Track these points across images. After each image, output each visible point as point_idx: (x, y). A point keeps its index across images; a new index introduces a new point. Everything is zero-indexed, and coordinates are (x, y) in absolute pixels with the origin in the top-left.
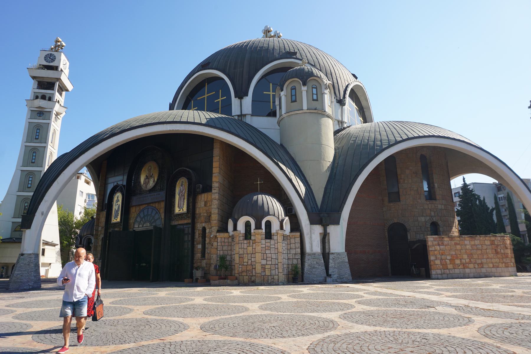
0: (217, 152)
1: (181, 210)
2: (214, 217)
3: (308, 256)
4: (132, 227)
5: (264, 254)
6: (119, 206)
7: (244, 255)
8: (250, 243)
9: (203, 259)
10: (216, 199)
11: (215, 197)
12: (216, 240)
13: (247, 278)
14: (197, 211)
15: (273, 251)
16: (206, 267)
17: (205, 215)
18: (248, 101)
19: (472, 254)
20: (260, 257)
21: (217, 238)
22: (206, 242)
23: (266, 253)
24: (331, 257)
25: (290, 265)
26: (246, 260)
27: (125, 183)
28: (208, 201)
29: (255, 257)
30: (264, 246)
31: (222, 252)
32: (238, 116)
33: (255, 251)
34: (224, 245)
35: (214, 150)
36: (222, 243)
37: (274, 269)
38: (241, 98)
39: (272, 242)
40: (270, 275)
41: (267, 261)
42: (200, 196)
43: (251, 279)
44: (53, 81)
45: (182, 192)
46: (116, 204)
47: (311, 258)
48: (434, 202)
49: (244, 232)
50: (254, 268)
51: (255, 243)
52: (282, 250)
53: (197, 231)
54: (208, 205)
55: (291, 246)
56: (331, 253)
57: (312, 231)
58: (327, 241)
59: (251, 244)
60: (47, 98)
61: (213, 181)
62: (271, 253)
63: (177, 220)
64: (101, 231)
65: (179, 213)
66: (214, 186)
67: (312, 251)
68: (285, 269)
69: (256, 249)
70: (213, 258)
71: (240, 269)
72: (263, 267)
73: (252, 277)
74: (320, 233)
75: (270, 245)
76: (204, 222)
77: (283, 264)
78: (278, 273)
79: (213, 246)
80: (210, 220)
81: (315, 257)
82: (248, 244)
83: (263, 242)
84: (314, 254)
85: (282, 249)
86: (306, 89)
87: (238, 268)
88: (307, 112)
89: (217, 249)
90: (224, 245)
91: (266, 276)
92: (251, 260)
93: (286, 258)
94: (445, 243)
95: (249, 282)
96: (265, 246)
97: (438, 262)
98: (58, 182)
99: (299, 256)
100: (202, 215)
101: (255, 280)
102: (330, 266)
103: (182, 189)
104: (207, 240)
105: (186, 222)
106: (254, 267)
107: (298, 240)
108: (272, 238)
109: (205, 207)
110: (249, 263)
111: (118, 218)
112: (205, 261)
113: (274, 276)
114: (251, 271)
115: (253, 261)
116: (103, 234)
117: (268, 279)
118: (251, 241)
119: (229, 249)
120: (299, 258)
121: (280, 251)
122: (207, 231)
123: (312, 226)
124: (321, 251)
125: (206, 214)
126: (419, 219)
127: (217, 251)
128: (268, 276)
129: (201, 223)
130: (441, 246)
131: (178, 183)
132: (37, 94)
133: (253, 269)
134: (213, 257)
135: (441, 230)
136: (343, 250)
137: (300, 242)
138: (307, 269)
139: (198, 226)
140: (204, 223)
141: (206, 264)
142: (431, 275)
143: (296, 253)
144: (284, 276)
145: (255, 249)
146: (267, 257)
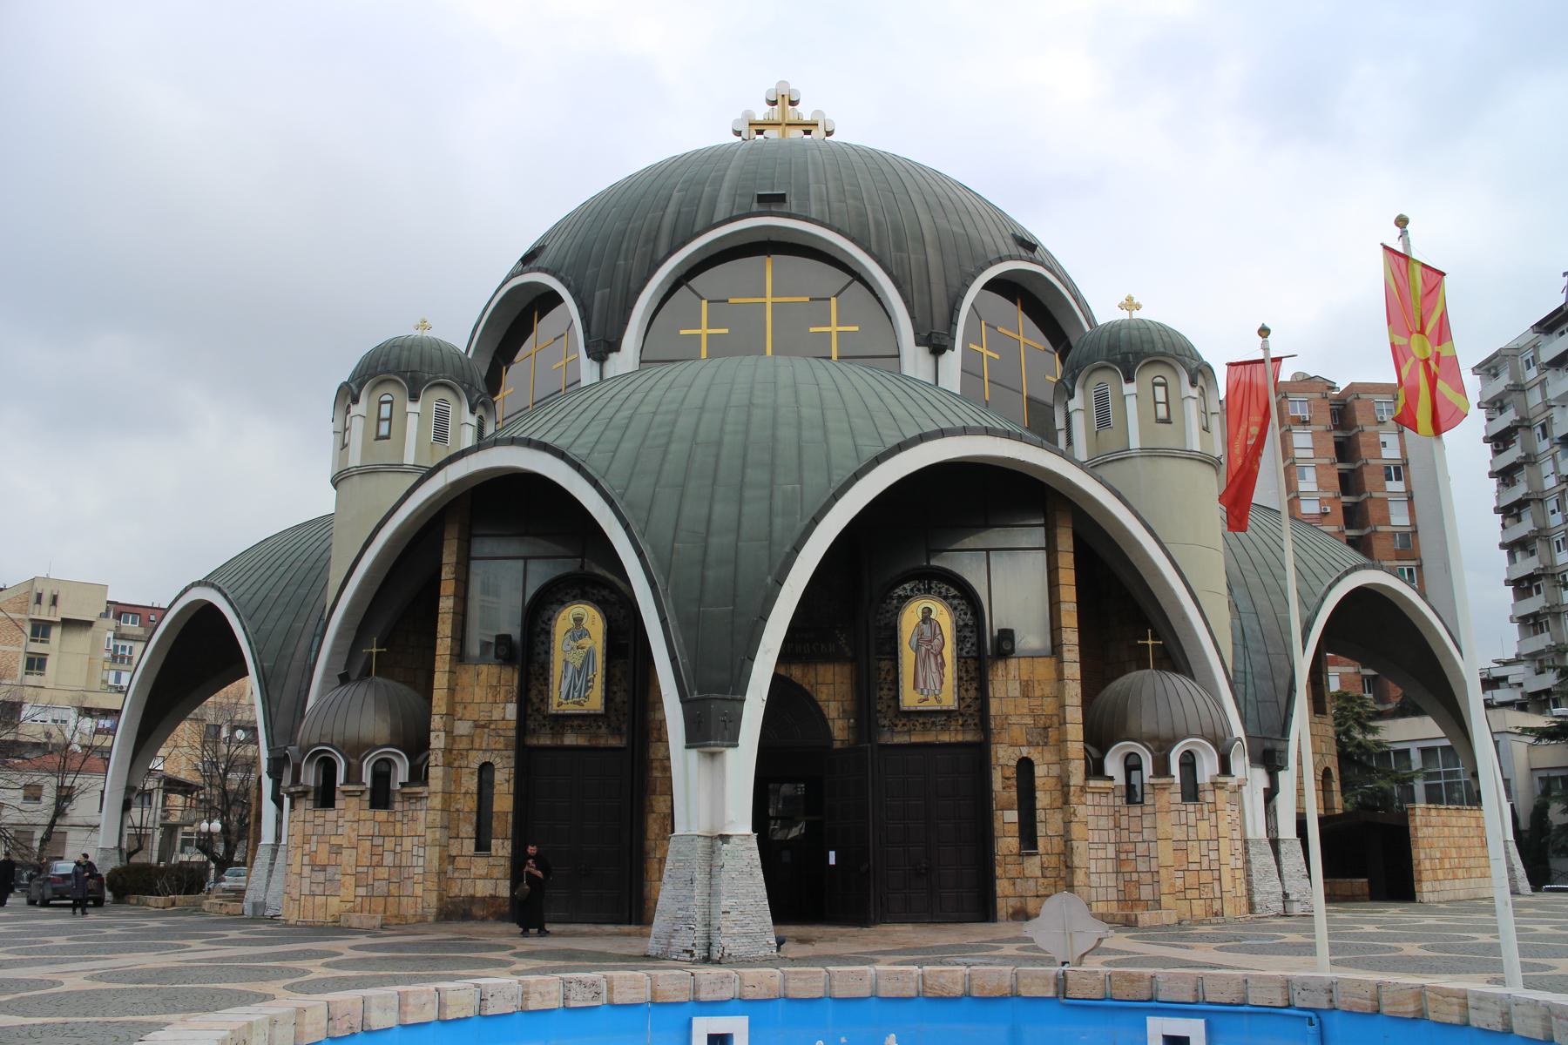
1: (931, 698)
6: (589, 656)
8: (1202, 810)
9: (1031, 854)
11: (1072, 674)
12: (1083, 799)
16: (1044, 877)
19: (1460, 847)
21: (1086, 792)
22: (1039, 804)
24: (1283, 848)
26: (1194, 857)
28: (1036, 683)
31: (1097, 832)
33: (1218, 833)
35: (1058, 531)
38: (937, 350)
42: (1001, 665)
43: (1211, 906)
45: (931, 641)
46: (572, 643)
53: (999, 768)
54: (1036, 695)
58: (1271, 808)
59: (1206, 813)
63: (909, 732)
64: (471, 737)
65: (919, 708)
71: (1179, 882)
74: (1264, 789)
76: (1025, 744)
79: (1076, 816)
80: (1047, 737)
82: (1198, 815)
87: (1170, 879)
97: (1427, 864)
98: (790, 585)
100: (1013, 720)
102: (1284, 872)
104: (1042, 799)
105: (945, 738)
106: (1216, 874)
109: (1027, 699)
110: (1205, 865)
111: (588, 697)
112: (1037, 859)
116: (434, 749)
118: (1205, 807)
119: (1111, 825)
122: (1040, 771)
123: (1253, 769)
125: (1029, 721)
129: (1011, 746)
135: (1334, 789)
139: (1001, 753)
141: (1042, 867)
142: (1417, 894)
145: (1217, 826)
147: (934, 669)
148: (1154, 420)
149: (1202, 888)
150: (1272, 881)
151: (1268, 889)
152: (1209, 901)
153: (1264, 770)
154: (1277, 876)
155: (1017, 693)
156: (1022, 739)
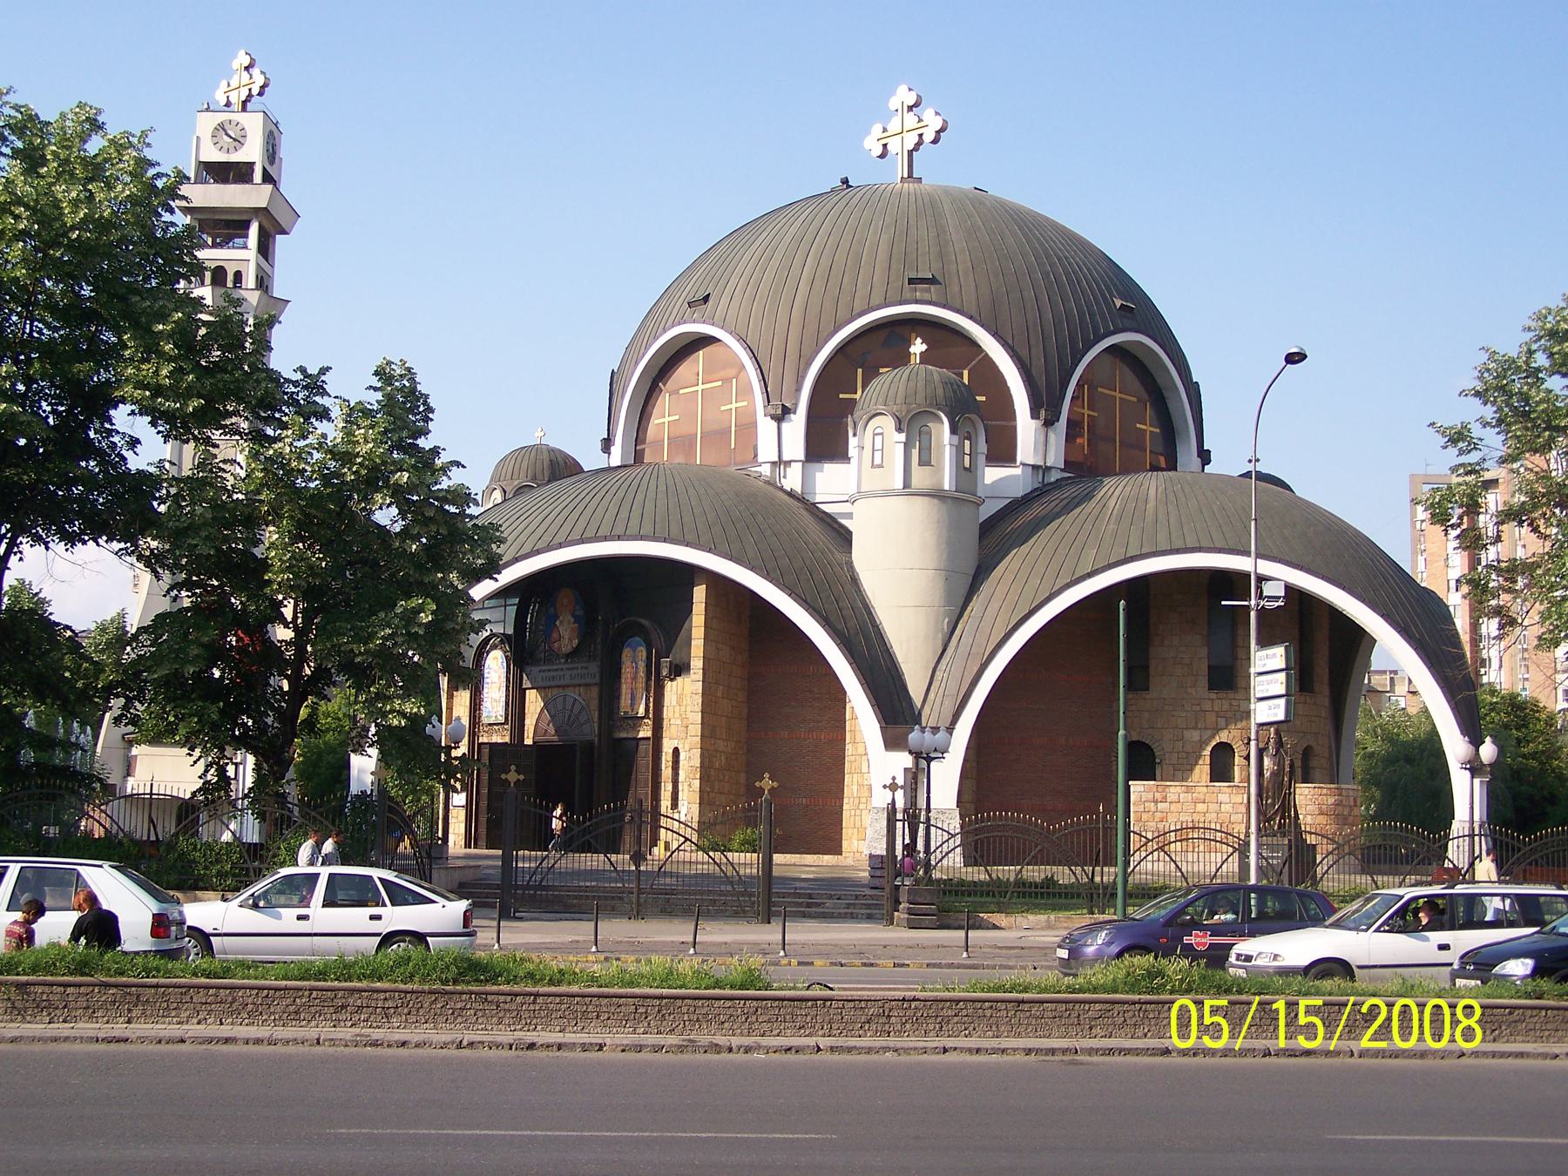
0: (700, 593)
4: (531, 735)
14: (666, 713)
18: (796, 427)
27: (510, 631)
32: (773, 463)
44: (245, 217)
48: (1231, 695)
60: (230, 278)
86: (904, 440)
94: (1171, 797)
122: (682, 756)
125: (679, 722)
126: (1187, 734)
130: (1159, 804)
131: (627, 654)
136: (954, 805)
155: (674, 703)
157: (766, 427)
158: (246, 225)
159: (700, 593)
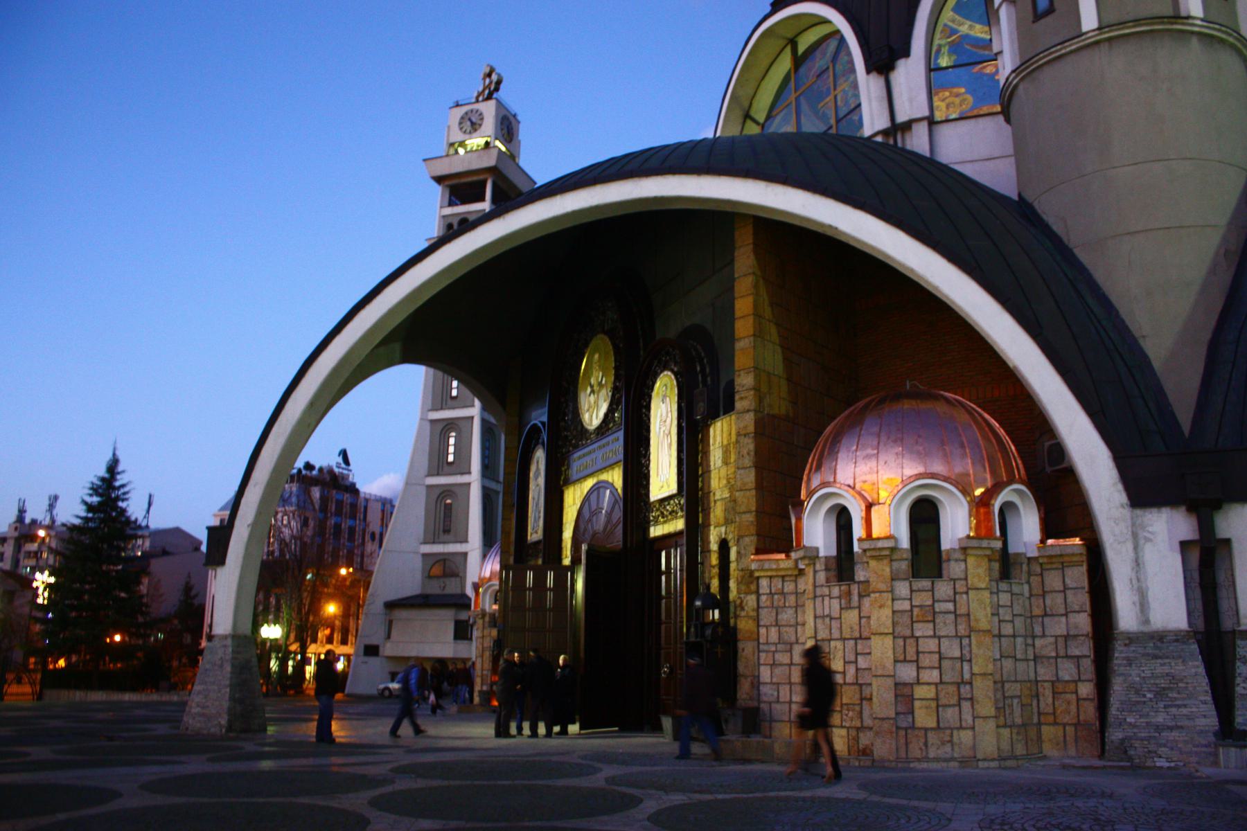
0: (745, 261)
2: (745, 501)
3: (1126, 645)
5: (908, 641)
7: (833, 643)
8: (849, 593)
10: (748, 434)
11: (745, 427)
12: (753, 587)
13: (842, 737)
15: (946, 628)
17: (724, 496)
20: (890, 654)
23: (918, 634)
25: (1046, 684)
29: (868, 651)
30: (906, 605)
31: (773, 630)
32: (885, 133)
34: (781, 604)
35: (736, 254)
36: (776, 597)
37: (954, 701)
39: (943, 589)
40: (932, 729)
41: (918, 668)
43: (857, 739)
44: (481, 177)
45: (665, 421)
47: (1148, 655)
49: (833, 552)
50: (869, 697)
51: (869, 595)
52: (990, 622)
55: (1048, 602)
56: (1241, 632)
57: (1142, 534)
58: (1221, 577)
59: (855, 598)
61: (736, 368)
62: (938, 634)
66: (739, 385)
67: (1147, 621)
68: (1016, 701)
69: (873, 618)
70: (744, 654)
72: (904, 694)
73: (861, 735)
74: (1184, 545)
75: (929, 603)
77: (998, 677)
78: (974, 718)
79: (743, 609)
81: (1156, 647)
82: (843, 601)
83: (902, 588)
84: (1159, 637)
85: (996, 619)
88: (1098, 38)
89: (757, 620)
90: (781, 604)
91: (916, 732)
92: (856, 662)
93: (1019, 656)
95: (849, 751)
96: (908, 608)
99: (1084, 648)
101: (872, 745)
103: (664, 415)
106: (866, 692)
107: (1078, 576)
108: (945, 572)
113: (955, 732)
114: (857, 708)
115: (863, 667)
117: (926, 744)
118: (855, 589)
120: (1086, 656)
121: (984, 624)
123: (1138, 512)
124: (1190, 623)
127: (756, 630)
128: (926, 730)
132: (450, 220)
133: (864, 702)
134: (746, 651)
137: (1086, 584)
138: (1122, 703)
140: (722, 525)
143: (1071, 633)
144: (1006, 732)
145: (869, 617)
146: (918, 653)
147: (667, 452)
148: (1030, 17)
149: (845, 712)
150: (1179, 706)
151: (1160, 719)
152: (853, 733)
153: (1183, 508)
154: (1209, 698)
155: (719, 463)
156: (722, 520)
157: (868, 86)
158: (484, 184)
159: (745, 261)
